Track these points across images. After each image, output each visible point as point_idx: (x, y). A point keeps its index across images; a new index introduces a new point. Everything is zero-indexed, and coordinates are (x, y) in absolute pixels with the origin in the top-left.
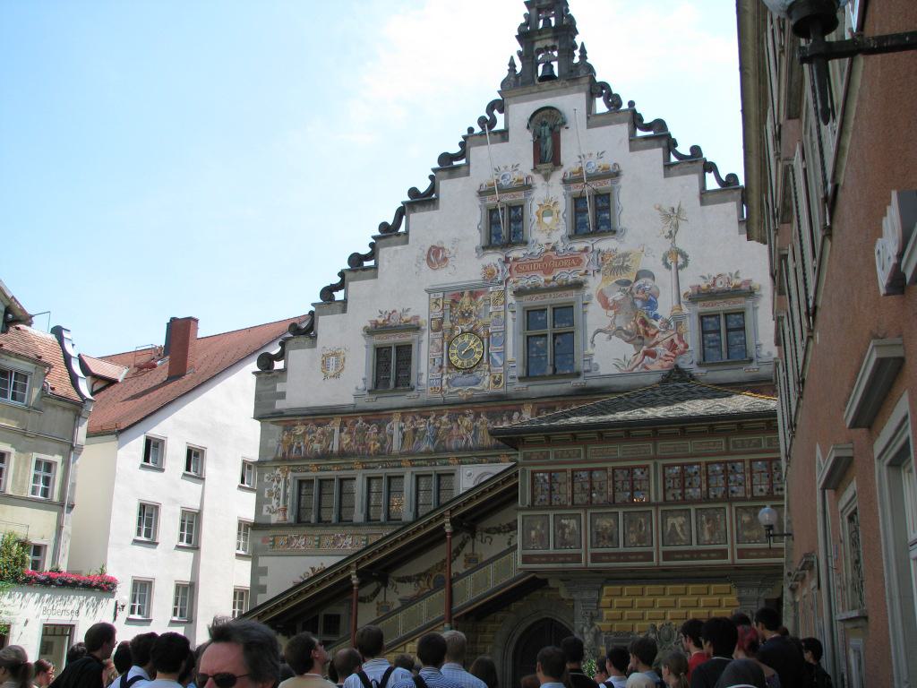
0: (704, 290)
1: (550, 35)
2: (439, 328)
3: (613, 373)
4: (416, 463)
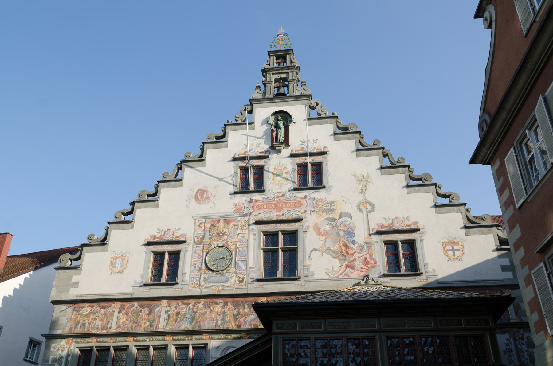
3: (324, 278)
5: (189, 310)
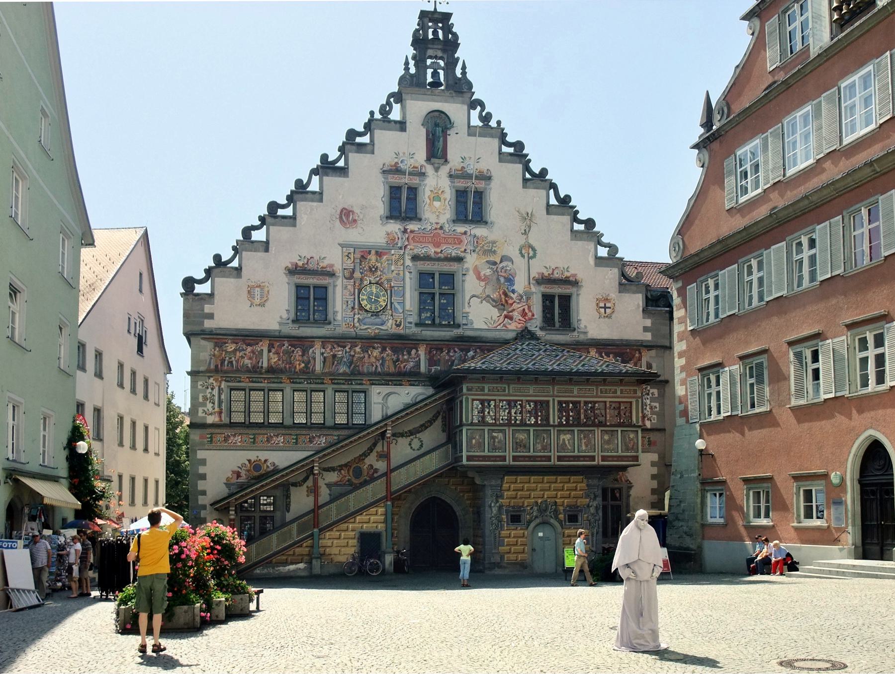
0: (546, 277)
1: (440, 47)
2: (351, 277)
4: (336, 381)
5: (346, 353)
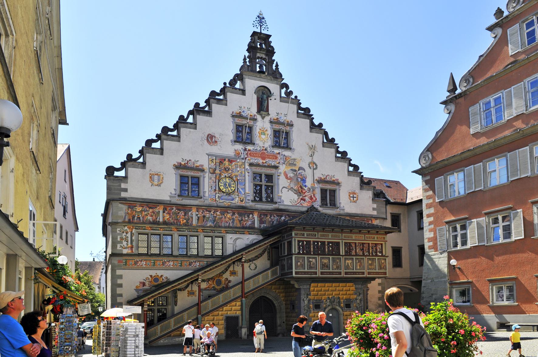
1: (264, 52)
2: (214, 172)
4: (205, 231)
5: (211, 215)
